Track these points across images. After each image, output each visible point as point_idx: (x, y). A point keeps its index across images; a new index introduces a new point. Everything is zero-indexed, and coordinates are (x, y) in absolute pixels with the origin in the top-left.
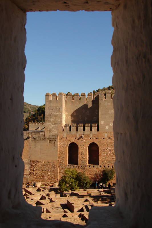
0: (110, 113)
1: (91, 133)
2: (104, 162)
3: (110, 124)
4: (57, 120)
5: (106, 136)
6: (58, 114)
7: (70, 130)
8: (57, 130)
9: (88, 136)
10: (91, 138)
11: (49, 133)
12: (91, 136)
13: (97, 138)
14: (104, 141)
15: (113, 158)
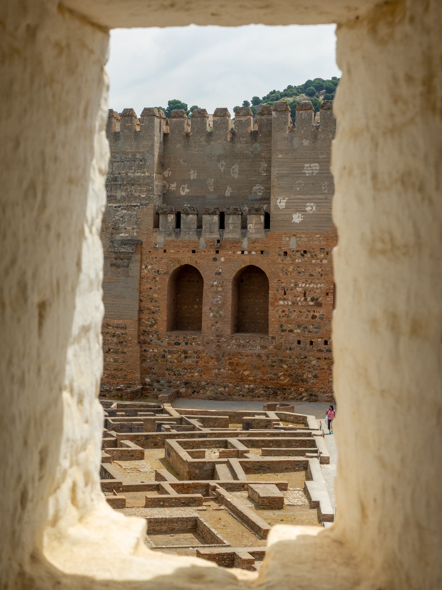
0: (308, 172)
1: (244, 235)
2: (284, 328)
3: (308, 209)
4: (137, 194)
5: (293, 244)
6: (139, 177)
7: (178, 225)
8: (135, 226)
9: (236, 243)
10: (243, 252)
11: (112, 234)
12: (245, 244)
13: (262, 252)
14: (286, 262)
15: (316, 314)
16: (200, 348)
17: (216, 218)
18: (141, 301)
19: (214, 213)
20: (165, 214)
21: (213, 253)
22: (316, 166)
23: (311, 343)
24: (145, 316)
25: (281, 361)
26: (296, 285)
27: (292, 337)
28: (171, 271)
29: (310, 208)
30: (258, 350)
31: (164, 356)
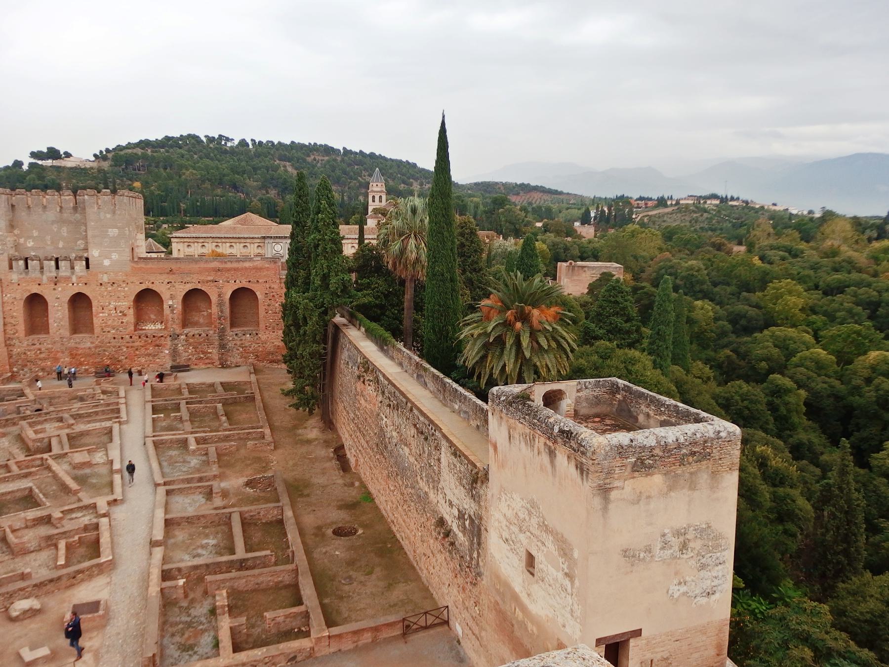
1: (73, 273)
3: (113, 257)
5: (105, 278)
9: (68, 279)
16: (50, 346)
17: (53, 263)
18: (4, 318)
19: (51, 260)
20: (16, 260)
21: (53, 285)
22: (116, 231)
23: (122, 338)
24: (9, 328)
25: (104, 350)
26: (110, 304)
27: (109, 335)
28: (24, 298)
29: (115, 256)
30: (88, 345)
31: (25, 353)
